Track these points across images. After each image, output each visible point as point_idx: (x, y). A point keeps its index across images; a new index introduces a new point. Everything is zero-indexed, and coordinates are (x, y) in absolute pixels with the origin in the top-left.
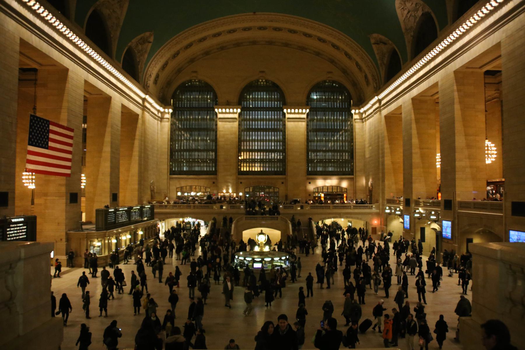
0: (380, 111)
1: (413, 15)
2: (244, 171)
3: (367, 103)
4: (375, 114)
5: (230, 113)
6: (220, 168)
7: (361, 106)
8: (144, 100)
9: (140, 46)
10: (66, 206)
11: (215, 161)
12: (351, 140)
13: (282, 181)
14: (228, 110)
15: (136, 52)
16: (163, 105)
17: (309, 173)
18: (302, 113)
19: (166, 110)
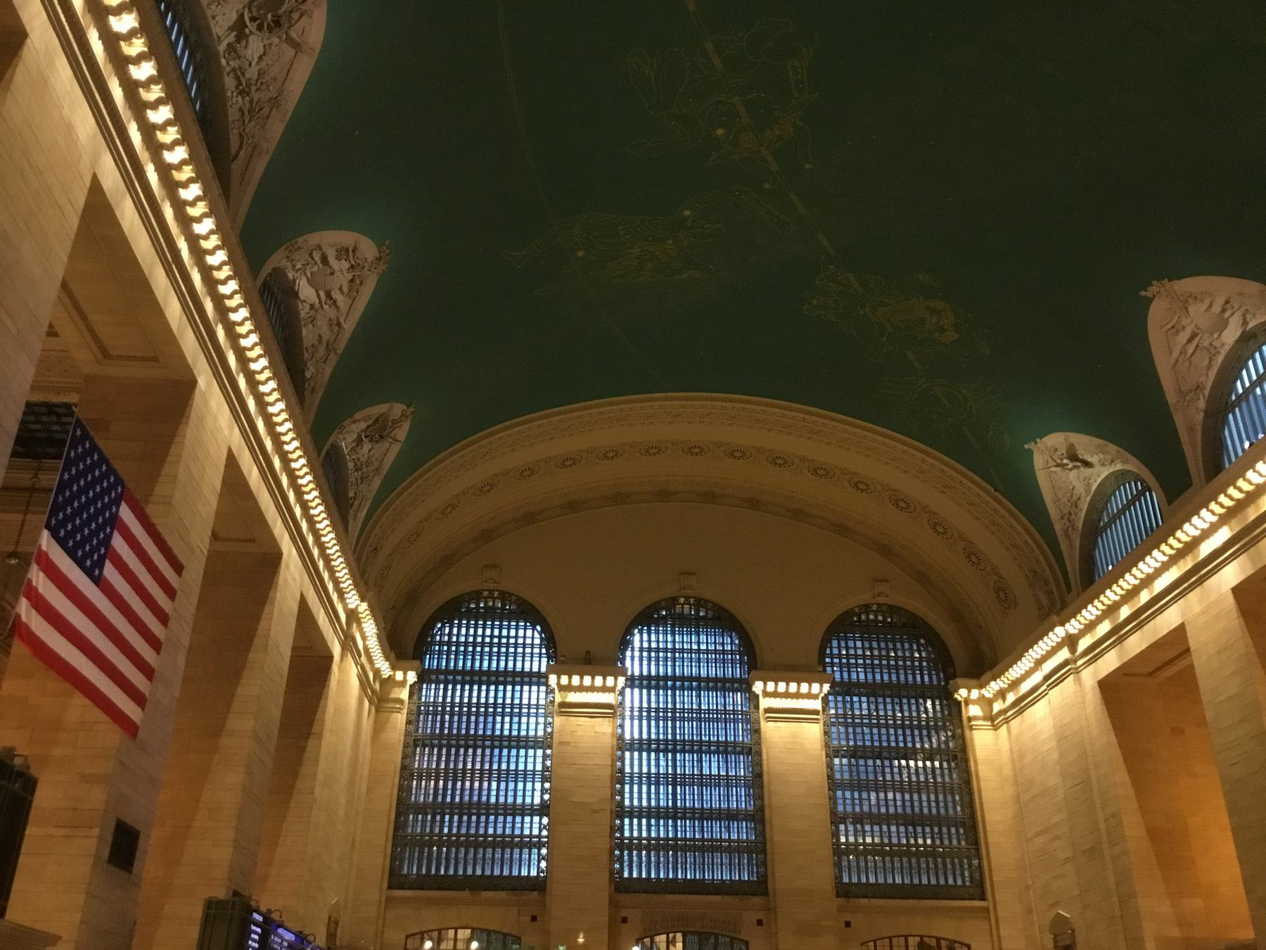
0: (1077, 671)
1: (1206, 344)
3: (1019, 658)
4: (1051, 687)
5: (592, 689)
7: (988, 674)
8: (353, 615)
9: (367, 446)
10: (94, 865)
12: (965, 785)
13: (760, 916)
14: (587, 680)
15: (351, 465)
16: (392, 655)
18: (809, 696)
19: (399, 676)
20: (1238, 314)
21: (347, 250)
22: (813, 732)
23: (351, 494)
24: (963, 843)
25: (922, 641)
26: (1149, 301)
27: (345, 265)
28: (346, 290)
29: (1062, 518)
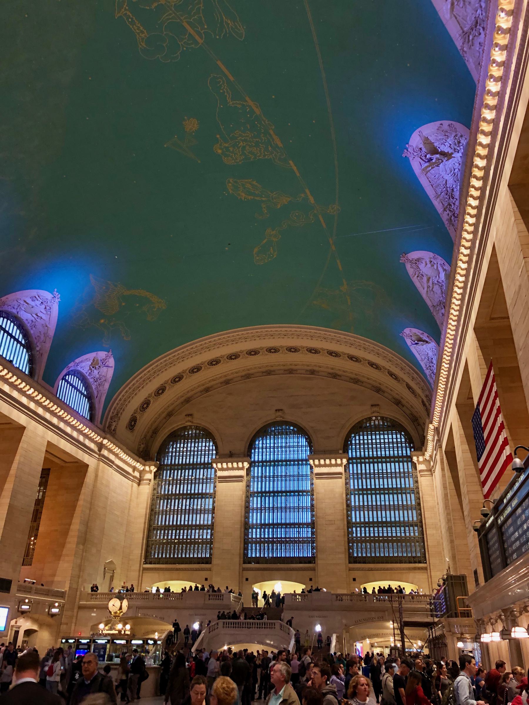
1: (436, 282)
2: (252, 557)
5: (233, 469)
6: (215, 552)
7: (423, 449)
8: (101, 446)
9: (96, 372)
11: (210, 542)
15: (91, 380)
16: (141, 460)
17: (353, 560)
18: (336, 465)
19: (147, 468)
20: (439, 266)
21: (35, 297)
22: (338, 484)
23: (95, 393)
24: (417, 534)
25: (403, 433)
26: (404, 265)
27: (38, 303)
28: (45, 312)
29: (427, 369)
